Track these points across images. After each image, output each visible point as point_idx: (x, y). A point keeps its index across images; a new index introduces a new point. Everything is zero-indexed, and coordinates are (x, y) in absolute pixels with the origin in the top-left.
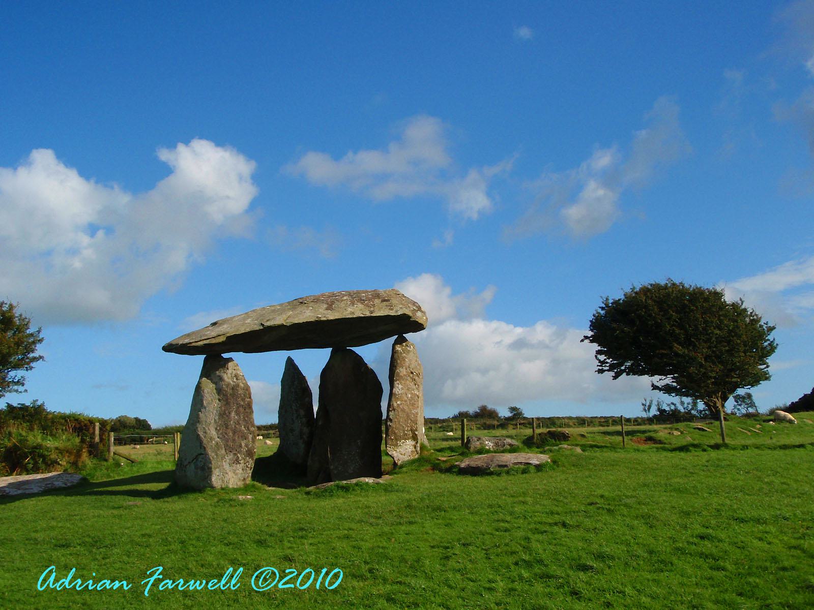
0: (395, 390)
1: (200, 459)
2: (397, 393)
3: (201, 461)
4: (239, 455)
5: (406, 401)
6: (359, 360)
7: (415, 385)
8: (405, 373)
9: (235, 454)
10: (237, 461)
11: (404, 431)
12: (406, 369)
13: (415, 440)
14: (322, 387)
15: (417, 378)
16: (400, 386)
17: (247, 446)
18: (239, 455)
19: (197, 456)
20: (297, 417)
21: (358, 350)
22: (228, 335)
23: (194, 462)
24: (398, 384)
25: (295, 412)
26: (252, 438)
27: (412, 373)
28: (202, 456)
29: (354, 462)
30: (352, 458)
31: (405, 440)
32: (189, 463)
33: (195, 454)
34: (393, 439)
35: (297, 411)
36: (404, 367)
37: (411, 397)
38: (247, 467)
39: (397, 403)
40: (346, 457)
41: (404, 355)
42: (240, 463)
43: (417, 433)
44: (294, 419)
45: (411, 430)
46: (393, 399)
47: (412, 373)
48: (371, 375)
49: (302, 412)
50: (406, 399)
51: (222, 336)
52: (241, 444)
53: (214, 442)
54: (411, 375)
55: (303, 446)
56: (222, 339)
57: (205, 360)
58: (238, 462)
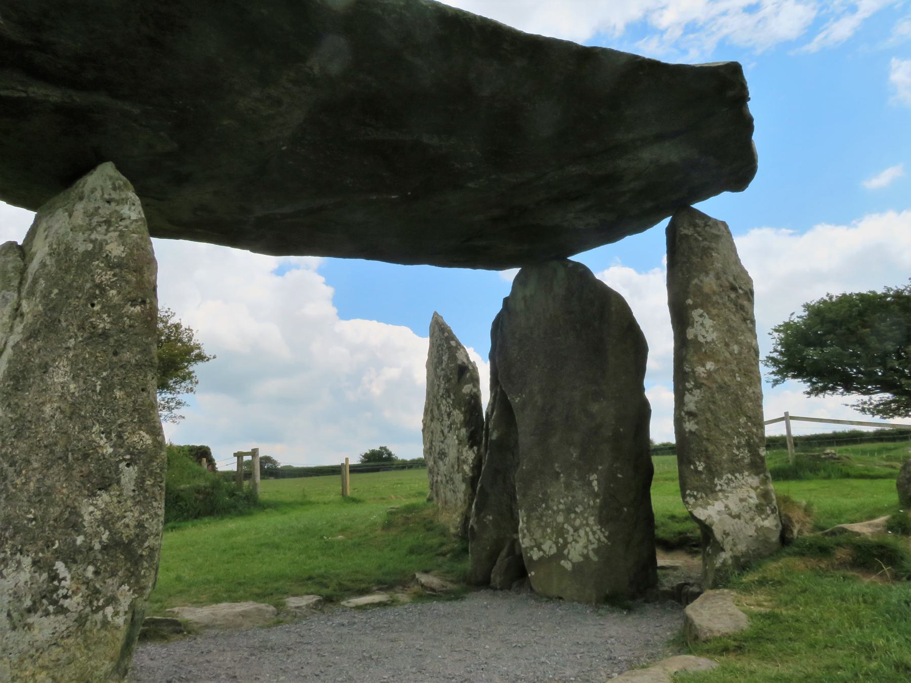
0: (690, 334)
4: (60, 566)
5: (726, 363)
12: (718, 277)
14: (497, 356)
15: (745, 303)
16: (708, 322)
18: (60, 566)
20: (450, 427)
24: (701, 316)
31: (733, 475)
34: (701, 473)
35: (449, 415)
36: (712, 275)
37: (740, 353)
39: (704, 366)
41: (705, 243)
42: (62, 610)
44: (446, 431)
45: (748, 444)
46: (691, 356)
49: (458, 416)
50: (727, 355)
52: (75, 512)
55: (463, 487)
58: (55, 603)
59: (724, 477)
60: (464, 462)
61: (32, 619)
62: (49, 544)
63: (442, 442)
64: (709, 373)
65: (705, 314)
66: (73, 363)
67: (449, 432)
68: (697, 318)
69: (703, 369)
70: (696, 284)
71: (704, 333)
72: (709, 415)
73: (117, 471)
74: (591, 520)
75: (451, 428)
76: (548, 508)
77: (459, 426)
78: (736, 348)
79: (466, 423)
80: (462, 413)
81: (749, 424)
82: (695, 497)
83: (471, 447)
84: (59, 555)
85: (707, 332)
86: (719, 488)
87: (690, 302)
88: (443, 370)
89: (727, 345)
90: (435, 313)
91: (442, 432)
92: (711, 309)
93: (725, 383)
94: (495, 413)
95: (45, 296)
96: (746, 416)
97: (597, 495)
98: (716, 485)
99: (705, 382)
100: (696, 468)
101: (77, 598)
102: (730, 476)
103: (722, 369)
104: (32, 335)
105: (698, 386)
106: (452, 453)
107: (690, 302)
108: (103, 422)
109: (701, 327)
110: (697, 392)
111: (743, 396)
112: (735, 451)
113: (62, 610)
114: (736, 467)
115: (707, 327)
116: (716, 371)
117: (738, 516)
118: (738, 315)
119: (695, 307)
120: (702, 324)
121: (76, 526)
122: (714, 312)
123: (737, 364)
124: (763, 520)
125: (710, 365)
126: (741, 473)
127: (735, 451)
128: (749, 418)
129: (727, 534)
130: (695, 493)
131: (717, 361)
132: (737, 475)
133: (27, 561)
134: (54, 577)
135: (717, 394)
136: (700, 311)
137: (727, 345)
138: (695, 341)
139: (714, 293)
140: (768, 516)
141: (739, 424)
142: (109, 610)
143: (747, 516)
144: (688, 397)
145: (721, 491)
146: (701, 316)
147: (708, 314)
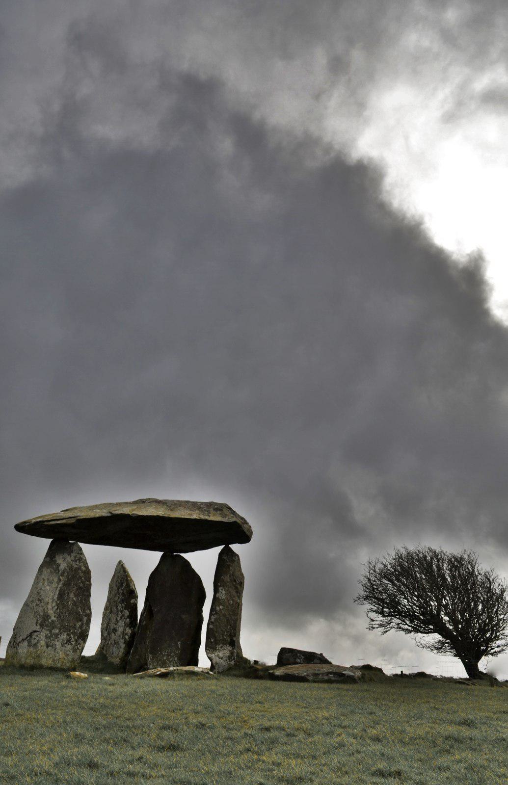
0: (217, 595)
1: (34, 637)
3: (34, 638)
4: (72, 635)
6: (187, 564)
9: (68, 635)
10: (69, 641)
12: (230, 576)
13: (232, 646)
15: (239, 586)
16: (224, 592)
17: (81, 627)
18: (72, 635)
19: (31, 633)
20: (121, 618)
21: (185, 556)
22: (78, 518)
23: (27, 639)
24: (222, 590)
25: (120, 612)
26: (87, 621)
28: (35, 634)
29: (172, 663)
30: (171, 659)
32: (23, 640)
33: (29, 632)
34: (212, 642)
35: (122, 612)
37: (233, 604)
38: (78, 649)
40: (165, 658)
43: (234, 639)
44: (118, 619)
48: (194, 579)
49: (127, 613)
51: (73, 519)
52: (75, 625)
53: (50, 620)
55: (123, 646)
56: (73, 521)
57: (52, 544)
60: (126, 634)
61: (65, 645)
62: (70, 631)
63: (116, 624)
64: (220, 609)
66: (74, 594)
67: (120, 620)
72: (217, 624)
73: (83, 618)
74: (176, 659)
75: (122, 618)
76: (161, 654)
77: (126, 617)
79: (130, 617)
80: (129, 612)
82: (209, 651)
83: (130, 628)
84: (72, 633)
87: (219, 584)
88: (122, 590)
89: (229, 601)
90: (120, 562)
91: (117, 619)
94: (145, 614)
95: (68, 577)
97: (178, 649)
101: (74, 642)
104: (64, 585)
105: (216, 613)
106: (120, 630)
107: (219, 584)
110: (215, 615)
113: (71, 644)
114: (224, 642)
117: (222, 658)
119: (221, 586)
121: (75, 628)
122: (227, 589)
126: (226, 644)
128: (231, 627)
129: (217, 664)
131: (224, 606)
133: (65, 634)
134: (71, 637)
137: (229, 601)
138: (218, 598)
142: (79, 646)
144: (212, 617)
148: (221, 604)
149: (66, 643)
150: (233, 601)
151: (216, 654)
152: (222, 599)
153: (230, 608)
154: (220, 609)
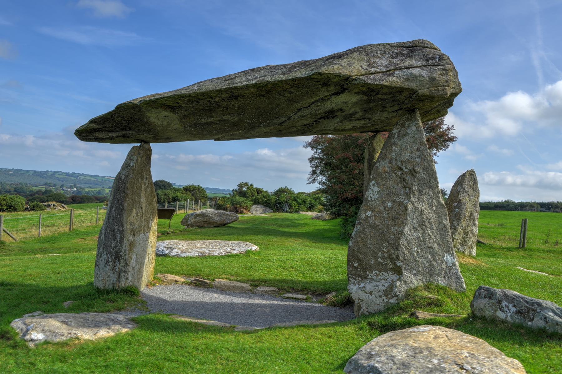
2: (369, 199)
5: (380, 212)
7: (405, 187)
8: (386, 169)
11: (376, 257)
12: (391, 162)
13: (399, 275)
16: (376, 189)
17: (116, 246)
24: (374, 185)
27: (400, 169)
31: (380, 272)
34: (356, 268)
37: (392, 207)
39: (365, 213)
47: (400, 169)
50: (382, 208)
54: (399, 173)
59: (374, 272)
64: (367, 218)
65: (376, 184)
68: (372, 187)
69: (364, 215)
70: (377, 166)
71: (372, 195)
78: (389, 205)
81: (390, 247)
85: (373, 194)
86: (370, 277)
92: (380, 181)
93: (374, 224)
96: (388, 243)
98: (368, 275)
99: (362, 222)
100: (353, 265)
102: (378, 272)
103: (375, 216)
105: (359, 224)
108: (117, 223)
109: (371, 192)
110: (359, 226)
111: (388, 232)
112: (380, 260)
114: (382, 268)
115: (374, 192)
116: (370, 217)
117: (371, 293)
118: (400, 185)
120: (372, 190)
122: (382, 183)
123: (388, 214)
124: (389, 299)
125: (369, 213)
127: (380, 260)
128: (390, 244)
130: (354, 277)
132: (384, 273)
134: (108, 258)
135: (367, 230)
136: (374, 182)
137: (384, 202)
138: (367, 200)
139: (385, 172)
140: (393, 297)
141: (383, 246)
143: (378, 294)
145: (371, 279)
146: (374, 185)
147: (377, 184)
148: (369, 209)
149: (106, 264)
150: (394, 202)
151: (362, 285)
152: (371, 201)
153: (385, 215)
154: (367, 218)
